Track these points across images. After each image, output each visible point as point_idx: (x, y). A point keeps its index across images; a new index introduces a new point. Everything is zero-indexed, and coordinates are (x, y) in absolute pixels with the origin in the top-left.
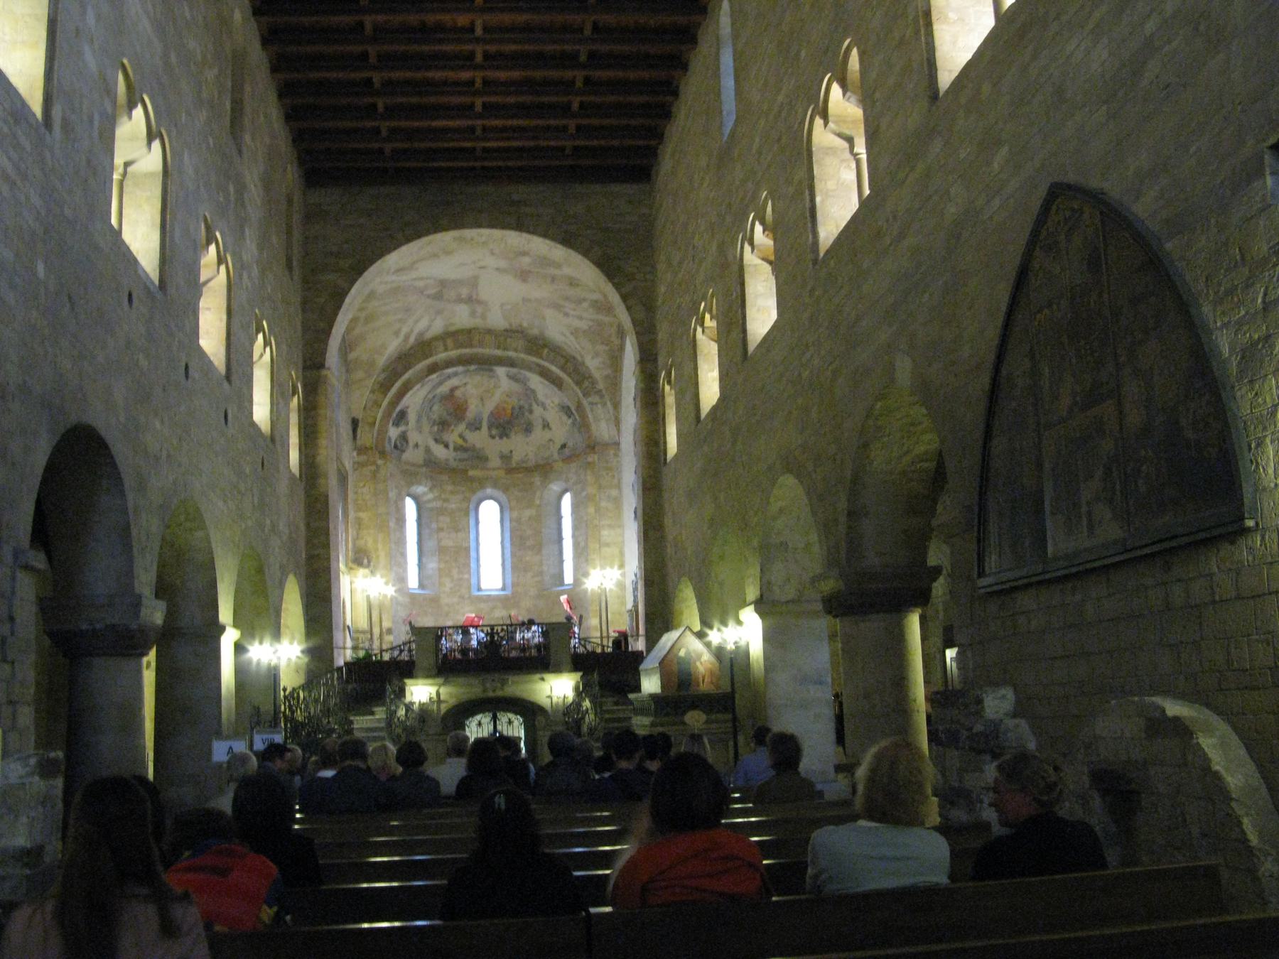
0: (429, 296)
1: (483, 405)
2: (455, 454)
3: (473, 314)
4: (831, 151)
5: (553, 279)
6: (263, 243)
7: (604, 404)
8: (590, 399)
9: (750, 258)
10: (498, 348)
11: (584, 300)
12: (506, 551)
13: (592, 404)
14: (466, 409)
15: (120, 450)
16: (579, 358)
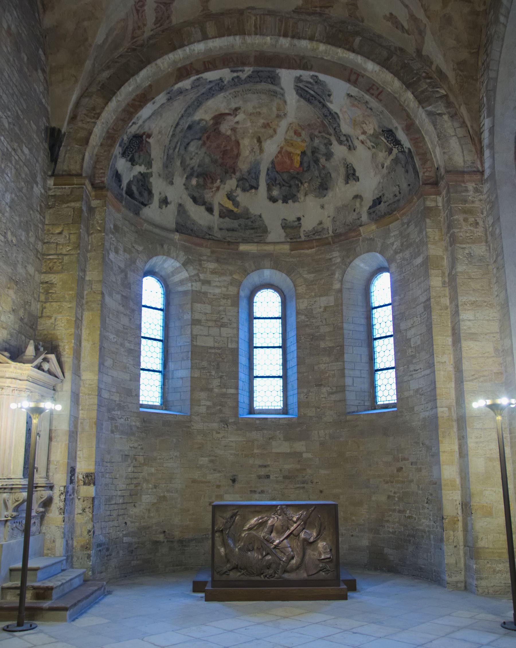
1: (261, 150)
2: (221, 220)
7: (453, 116)
8: (429, 108)
10: (285, 36)
12: (289, 357)
14: (238, 155)
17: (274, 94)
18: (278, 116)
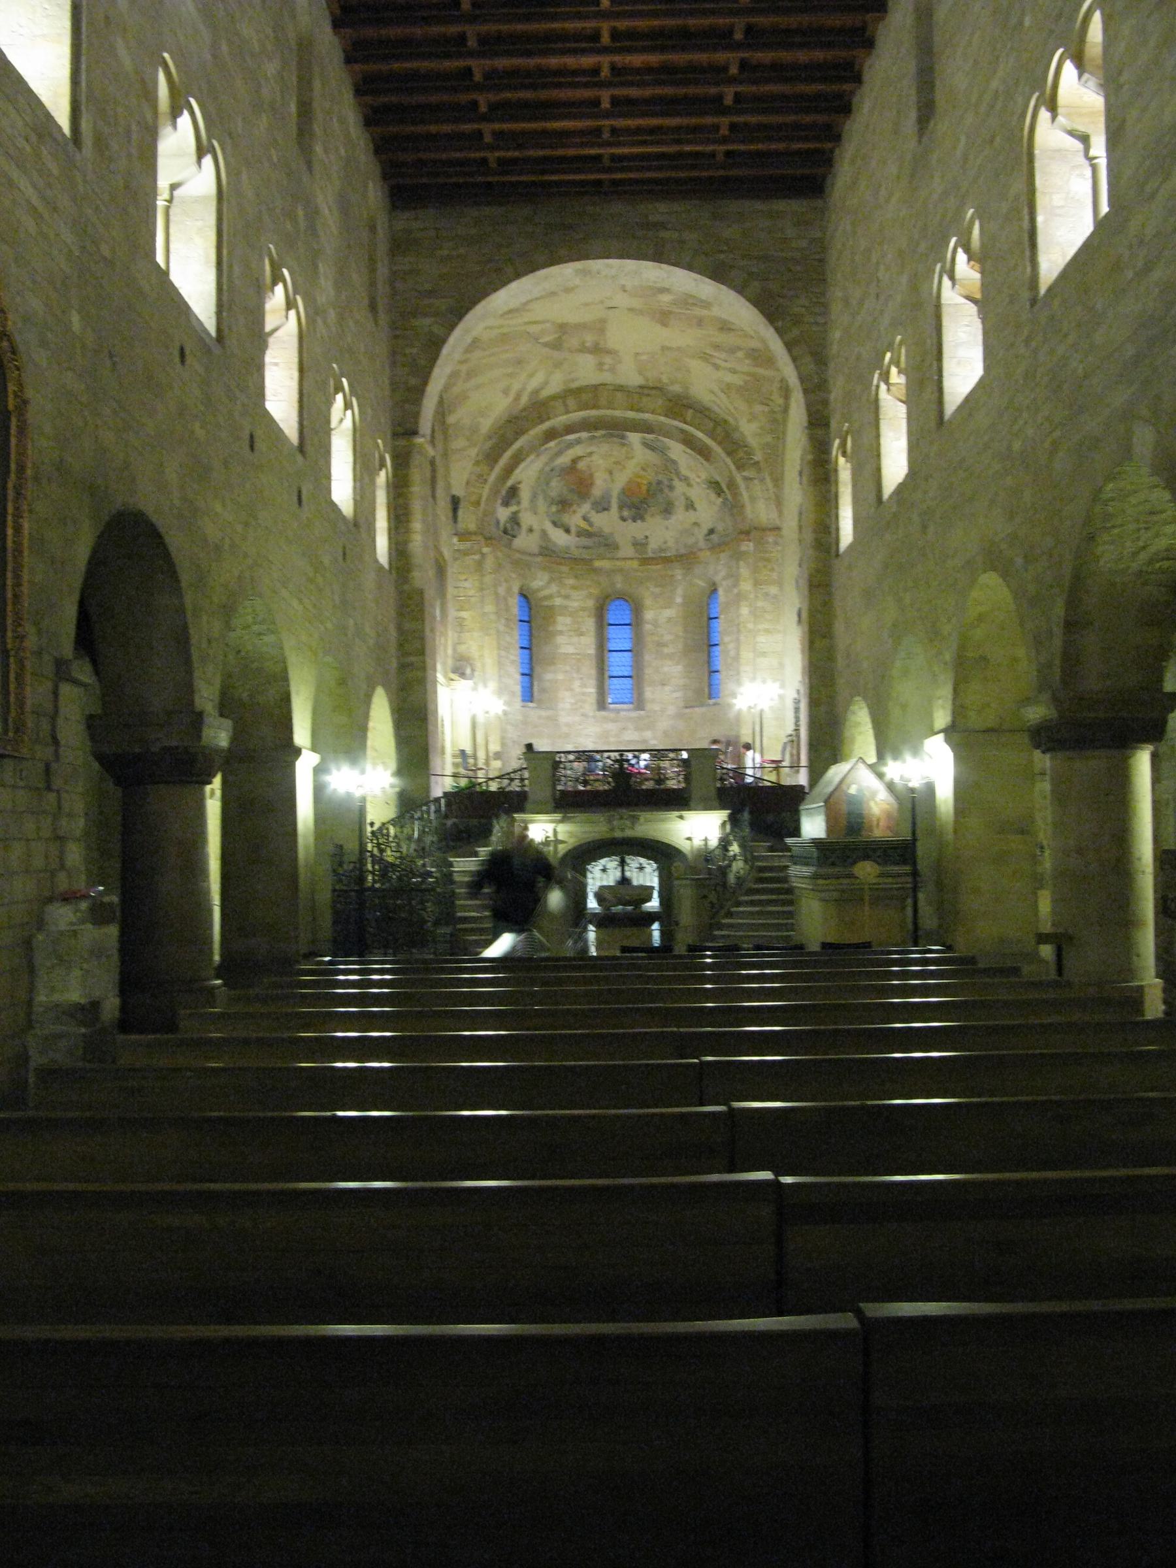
0: (546, 345)
1: (613, 481)
3: (600, 366)
4: (1059, 153)
5: (700, 322)
6: (342, 281)
7: (762, 480)
8: (745, 474)
9: (950, 296)
11: (739, 348)
13: (746, 479)
14: (592, 484)
15: (176, 541)
16: (731, 420)
17: (623, 445)
18: (627, 458)
